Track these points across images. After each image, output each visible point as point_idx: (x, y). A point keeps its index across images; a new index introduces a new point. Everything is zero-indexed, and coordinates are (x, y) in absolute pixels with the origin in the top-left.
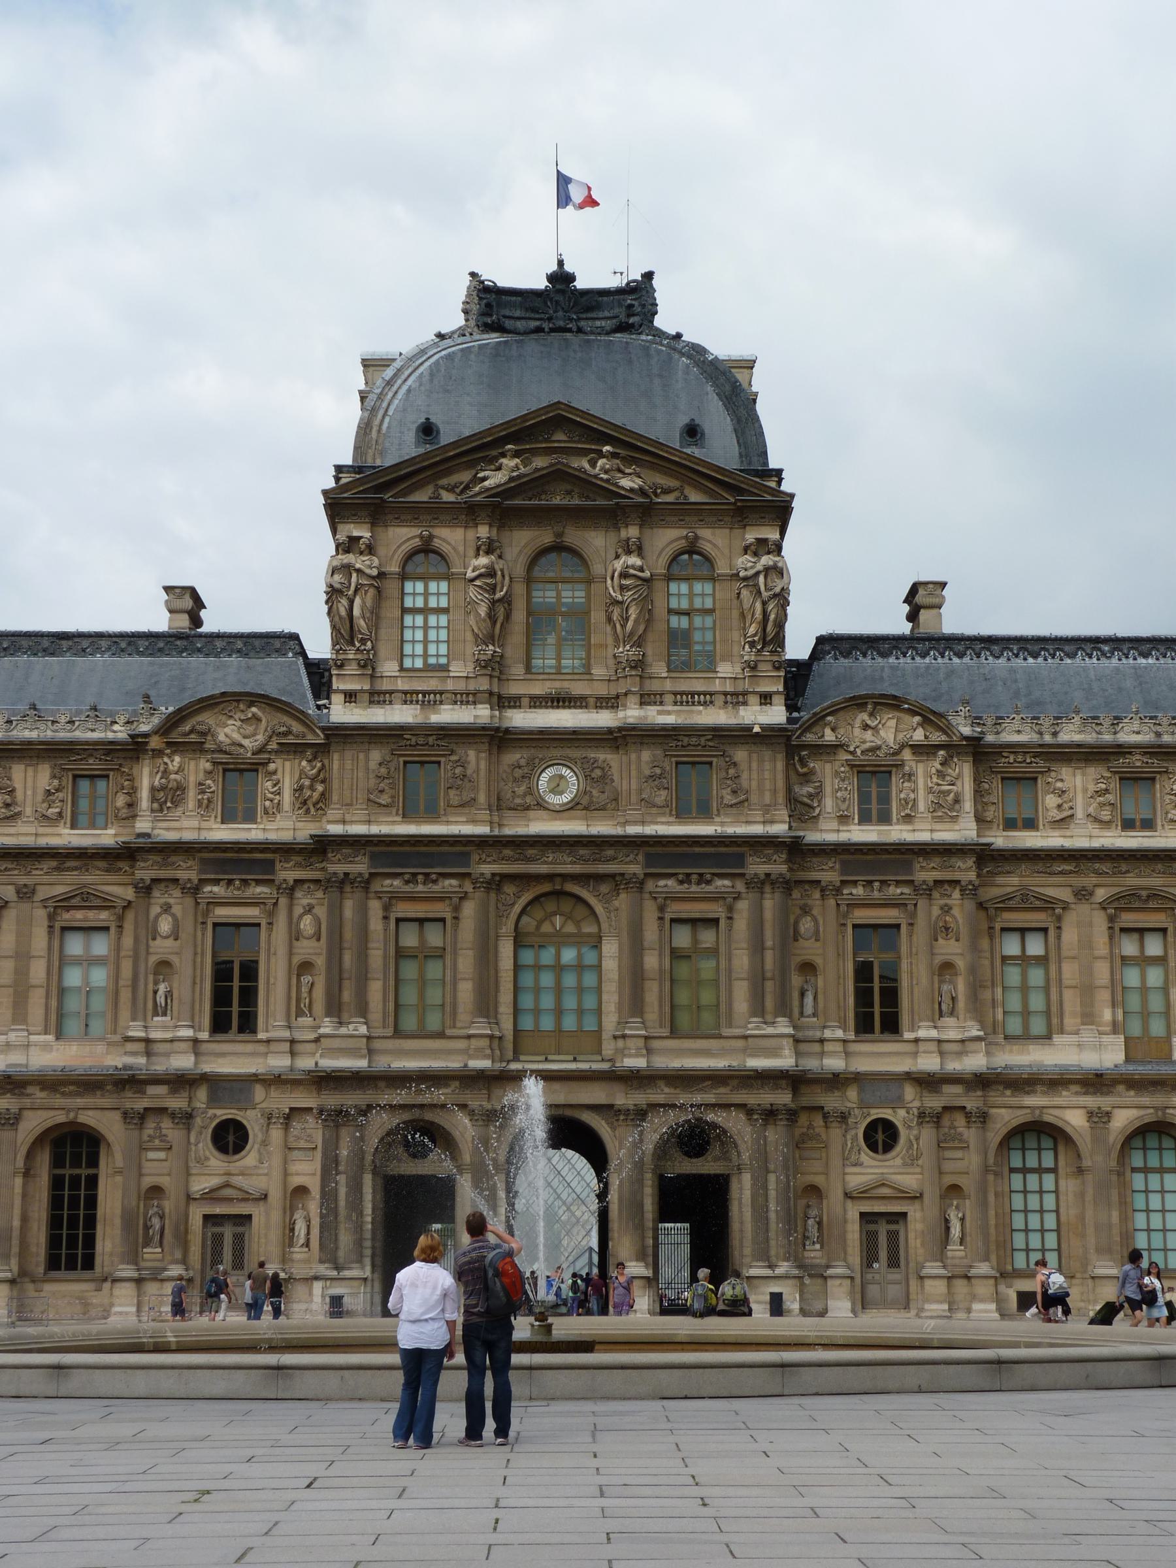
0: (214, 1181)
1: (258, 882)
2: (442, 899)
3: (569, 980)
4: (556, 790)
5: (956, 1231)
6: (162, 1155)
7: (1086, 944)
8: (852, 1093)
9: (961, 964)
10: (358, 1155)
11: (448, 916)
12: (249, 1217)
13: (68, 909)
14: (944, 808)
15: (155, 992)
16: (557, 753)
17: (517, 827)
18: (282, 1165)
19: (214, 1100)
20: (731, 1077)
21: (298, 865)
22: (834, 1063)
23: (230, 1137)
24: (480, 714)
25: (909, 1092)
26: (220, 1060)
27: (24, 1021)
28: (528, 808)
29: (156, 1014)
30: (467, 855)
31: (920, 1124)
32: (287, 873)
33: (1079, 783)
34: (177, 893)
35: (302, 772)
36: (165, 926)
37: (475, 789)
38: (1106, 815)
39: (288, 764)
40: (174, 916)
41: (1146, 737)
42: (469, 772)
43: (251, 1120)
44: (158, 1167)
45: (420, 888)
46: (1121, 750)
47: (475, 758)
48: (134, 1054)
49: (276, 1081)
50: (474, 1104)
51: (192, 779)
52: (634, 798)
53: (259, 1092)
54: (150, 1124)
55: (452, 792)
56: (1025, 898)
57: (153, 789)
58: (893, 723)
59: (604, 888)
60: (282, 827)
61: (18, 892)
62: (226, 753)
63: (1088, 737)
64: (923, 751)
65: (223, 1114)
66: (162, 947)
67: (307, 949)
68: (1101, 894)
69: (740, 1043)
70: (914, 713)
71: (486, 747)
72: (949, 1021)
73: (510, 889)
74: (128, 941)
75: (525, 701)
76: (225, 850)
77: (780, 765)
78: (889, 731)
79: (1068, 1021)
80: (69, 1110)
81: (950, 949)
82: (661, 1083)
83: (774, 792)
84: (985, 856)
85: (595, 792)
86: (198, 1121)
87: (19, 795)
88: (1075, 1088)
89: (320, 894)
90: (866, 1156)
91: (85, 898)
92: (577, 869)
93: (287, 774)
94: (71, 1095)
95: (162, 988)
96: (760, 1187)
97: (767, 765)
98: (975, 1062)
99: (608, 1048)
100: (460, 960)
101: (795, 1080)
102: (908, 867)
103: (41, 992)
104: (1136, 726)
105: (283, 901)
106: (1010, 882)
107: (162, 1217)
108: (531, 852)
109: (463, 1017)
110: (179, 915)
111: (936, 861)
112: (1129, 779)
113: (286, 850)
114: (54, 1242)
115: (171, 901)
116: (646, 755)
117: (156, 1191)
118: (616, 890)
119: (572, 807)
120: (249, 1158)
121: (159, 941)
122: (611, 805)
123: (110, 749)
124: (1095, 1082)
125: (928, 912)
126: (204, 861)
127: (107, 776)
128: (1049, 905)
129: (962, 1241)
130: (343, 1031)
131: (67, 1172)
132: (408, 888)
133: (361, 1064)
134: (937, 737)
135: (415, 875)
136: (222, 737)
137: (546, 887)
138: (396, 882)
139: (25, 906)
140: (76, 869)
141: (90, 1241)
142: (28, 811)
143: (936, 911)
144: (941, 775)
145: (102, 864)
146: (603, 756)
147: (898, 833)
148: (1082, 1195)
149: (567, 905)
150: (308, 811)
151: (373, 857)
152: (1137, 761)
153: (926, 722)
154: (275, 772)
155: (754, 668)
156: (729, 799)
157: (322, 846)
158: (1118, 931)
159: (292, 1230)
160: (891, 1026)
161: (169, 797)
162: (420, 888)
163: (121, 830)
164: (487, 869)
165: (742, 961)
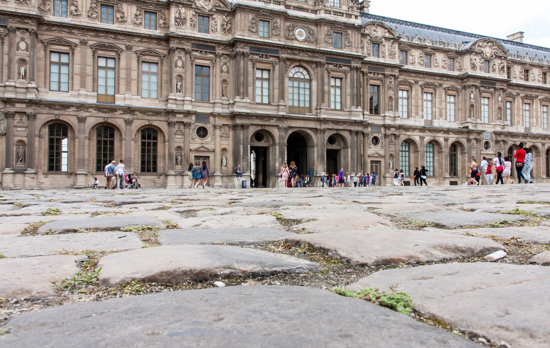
0: (198, 146)
1: (210, 53)
2: (270, 63)
3: (302, 91)
4: (301, 35)
5: (391, 166)
6: (181, 137)
7: (417, 95)
8: (369, 129)
9: (393, 97)
10: (245, 139)
11: (271, 69)
12: (209, 157)
13: (144, 55)
14: (392, 55)
15: (177, 85)
16: (301, 24)
18: (219, 142)
19: (197, 120)
20: (348, 122)
21: (223, 49)
23: (202, 132)
24: (281, 8)
25: (383, 130)
26: (199, 108)
27: (130, 91)
28: (293, 40)
29: (177, 92)
30: (278, 51)
31: (385, 138)
32: (219, 51)
34: (183, 53)
35: (224, 20)
36: (180, 63)
37: (280, 31)
38: (422, 63)
39: (219, 16)
40: (182, 60)
41: (430, 44)
42: (278, 26)
43: (209, 127)
44: (178, 140)
45: (264, 59)
46: (426, 47)
47: (279, 21)
48: (172, 104)
49: (219, 115)
50: (281, 126)
51: (188, 17)
52: (323, 40)
53: (212, 119)
54: (177, 127)
55: (274, 31)
56: (405, 82)
57: (176, 18)
58: (381, 31)
59: (314, 66)
61: (126, 47)
62: (199, 9)
63: (419, 42)
65: (200, 125)
66: (178, 70)
67: (225, 75)
68: (420, 83)
69: (348, 113)
70: (386, 29)
71: (283, 19)
72: (391, 112)
73: (288, 63)
74: (165, 68)
75: (292, 7)
76: (199, 41)
77: (359, 36)
78: (380, 33)
79: (413, 114)
80: (149, 120)
81: (391, 93)
82: (330, 123)
83: (358, 44)
85: (311, 38)
86: (192, 126)
87: (126, 15)
88: (418, 131)
89: (228, 59)
90: (372, 146)
91: (150, 52)
92: (308, 59)
93: (219, 19)
94: (150, 115)
95: (179, 84)
96: (352, 152)
97: (357, 36)
99: (314, 112)
100: (275, 82)
102: (383, 70)
103: (136, 82)
104: (429, 41)
105: (218, 60)
107: (181, 156)
108: (296, 52)
109: (276, 100)
110: (184, 60)
111: (390, 69)
112: (427, 54)
113: (220, 43)
114: (143, 163)
115: (182, 56)
116: (326, 28)
117: (179, 148)
118: (317, 67)
119: (305, 41)
120: (208, 139)
121: (178, 68)
122: (316, 41)
126: (192, 44)
127: (156, 13)
128: (410, 85)
129: (393, 168)
130: (242, 100)
131: (147, 141)
132: (260, 59)
133: (248, 111)
134: (391, 36)
135: (263, 55)
136: (198, 4)
137: (298, 64)
138: (257, 57)
139: (129, 52)
140: (146, 42)
141: (155, 163)
142: (129, 20)
143: (388, 83)
144: (392, 47)
145: (156, 42)
146: (313, 28)
147: (381, 60)
148: (417, 158)
149: (301, 70)
150: (225, 33)
151: (251, 48)
152: (429, 50)
153: (389, 32)
154: (215, 19)
155: (352, 8)
156: (347, 44)
157: (233, 44)
159: (222, 162)
161: (180, 21)
162: (264, 59)
163: (162, 31)
164: (284, 56)
165: (349, 90)
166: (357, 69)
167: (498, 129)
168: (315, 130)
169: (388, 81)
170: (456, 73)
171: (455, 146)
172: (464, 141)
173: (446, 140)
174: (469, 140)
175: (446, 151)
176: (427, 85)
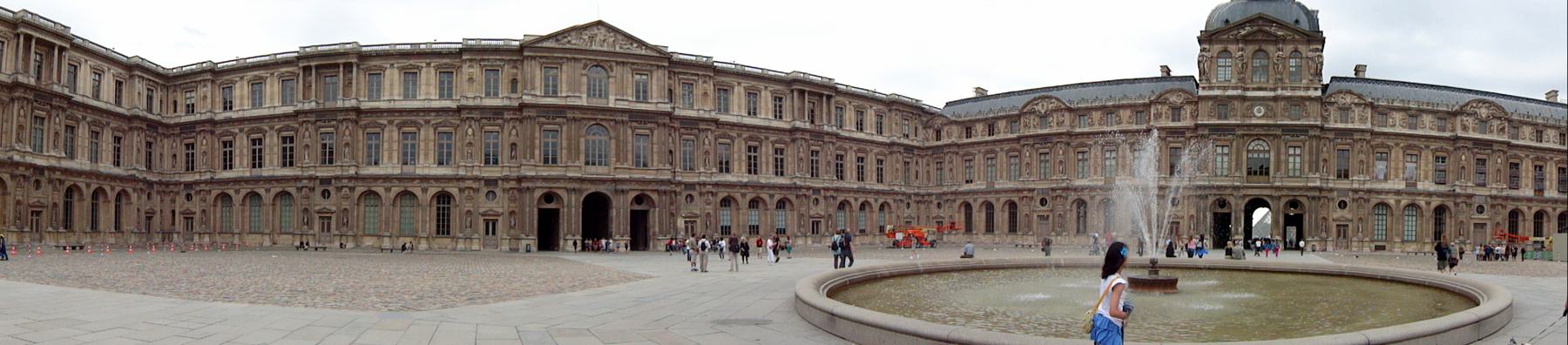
17: (1248, 122)
60: (1186, 122)
81: (1362, 157)
84: (1372, 133)
123: (1144, 105)
125: (1358, 146)
161: (1158, 116)
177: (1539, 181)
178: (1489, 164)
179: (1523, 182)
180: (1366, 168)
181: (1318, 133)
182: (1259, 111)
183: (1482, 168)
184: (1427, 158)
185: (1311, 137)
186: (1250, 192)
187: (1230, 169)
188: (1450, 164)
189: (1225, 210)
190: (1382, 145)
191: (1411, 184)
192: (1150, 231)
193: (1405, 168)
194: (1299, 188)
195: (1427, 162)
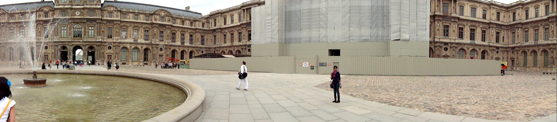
14: (117, 16)
22: (105, 41)
33: (131, 15)
64: (115, 11)
78: (112, 9)
81: (117, 30)
84: (121, 21)
98: (119, 41)
101: (101, 42)
106: (123, 24)
124: (131, 43)
128: (128, 27)
147: (113, 19)
158: (133, 29)
160: (111, 37)
166: (100, 23)
167: (166, 43)
168: (83, 45)
169: (115, 26)
170: (149, 22)
171: (146, 50)
172: (150, 47)
173: (142, 47)
174: (152, 48)
175: (142, 51)
176: (135, 26)
177: (183, 39)
178: (165, 33)
179: (177, 40)
180: (118, 34)
181: (100, 21)
182: (78, 13)
183: (162, 35)
184: (142, 31)
185: (97, 23)
186: (75, 43)
187: (67, 35)
188: (150, 33)
189: (65, 50)
190: (124, 26)
191: (135, 40)
192: (33, 59)
193: (133, 34)
194: (93, 42)
195: (141, 32)
